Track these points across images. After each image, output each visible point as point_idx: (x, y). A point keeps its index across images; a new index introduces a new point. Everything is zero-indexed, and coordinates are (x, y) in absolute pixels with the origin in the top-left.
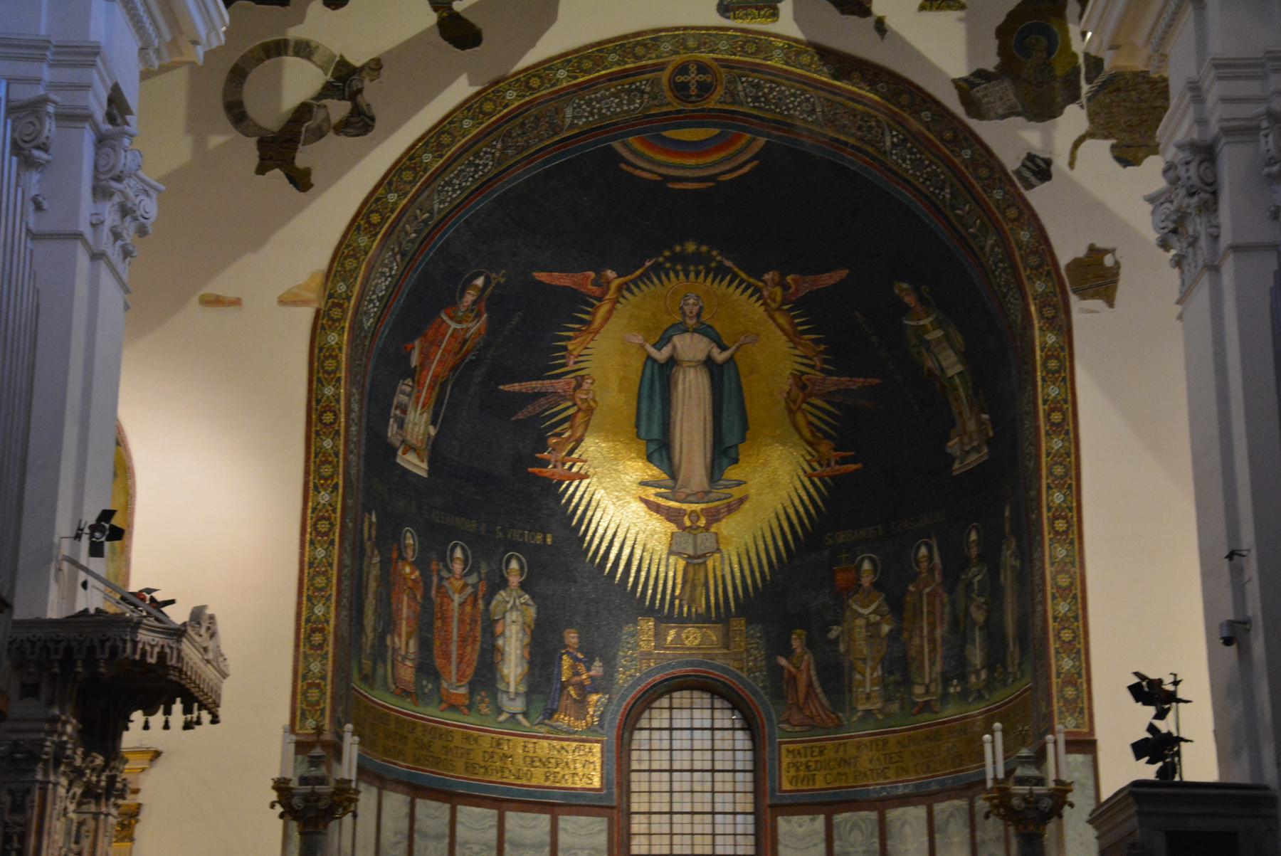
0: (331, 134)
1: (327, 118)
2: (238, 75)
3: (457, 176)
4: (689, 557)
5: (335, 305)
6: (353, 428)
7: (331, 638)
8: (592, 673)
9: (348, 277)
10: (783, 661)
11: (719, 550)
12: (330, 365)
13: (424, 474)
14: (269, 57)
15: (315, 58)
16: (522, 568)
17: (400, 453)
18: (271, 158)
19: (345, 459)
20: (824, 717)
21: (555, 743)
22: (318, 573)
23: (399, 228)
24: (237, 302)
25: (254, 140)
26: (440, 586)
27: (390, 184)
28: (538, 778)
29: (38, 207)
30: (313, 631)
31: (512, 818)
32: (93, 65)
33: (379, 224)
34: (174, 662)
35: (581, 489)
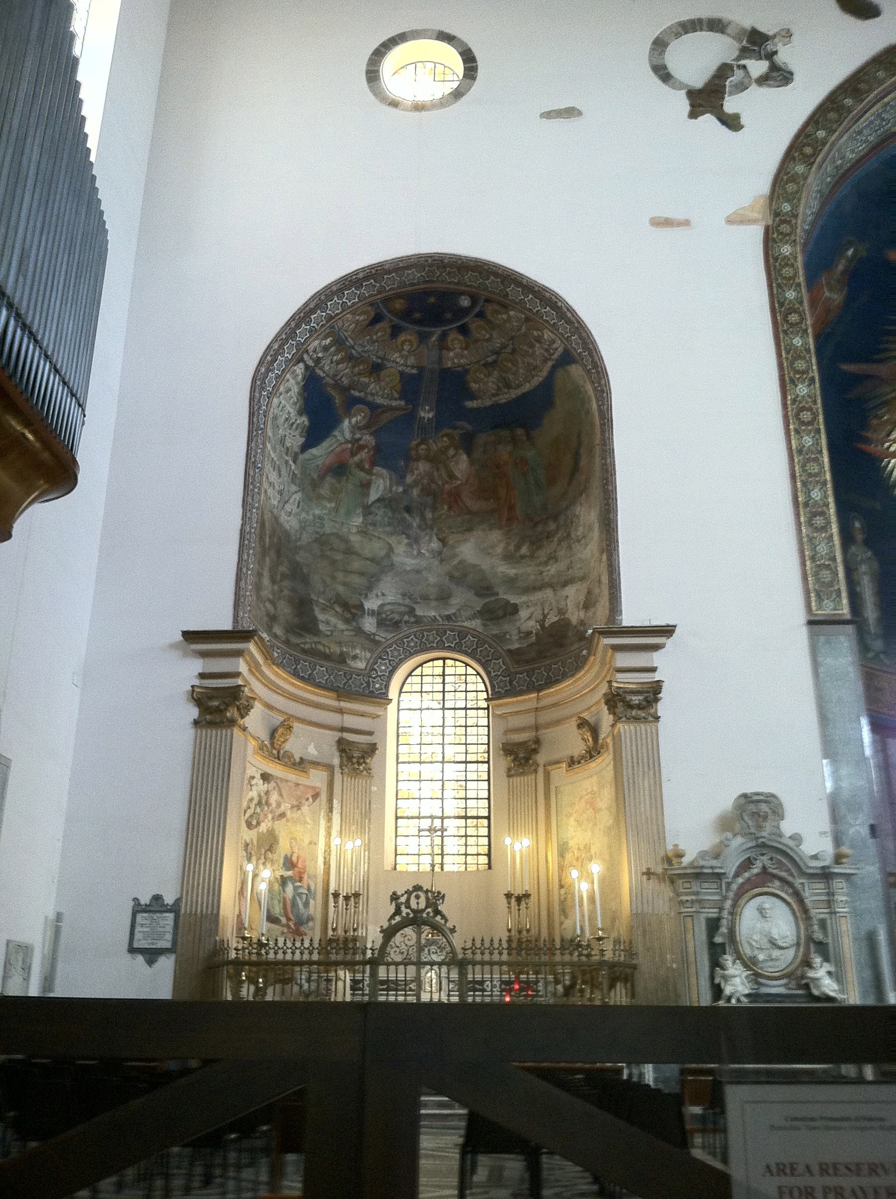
0: (754, 87)
2: (660, 45)
3: (868, 125)
7: (833, 519)
9: (792, 198)
12: (787, 272)
14: (686, 33)
15: (729, 31)
18: (701, 105)
22: (809, 460)
24: (686, 223)
25: (683, 93)
27: (817, 123)
30: (814, 515)
33: (812, 156)
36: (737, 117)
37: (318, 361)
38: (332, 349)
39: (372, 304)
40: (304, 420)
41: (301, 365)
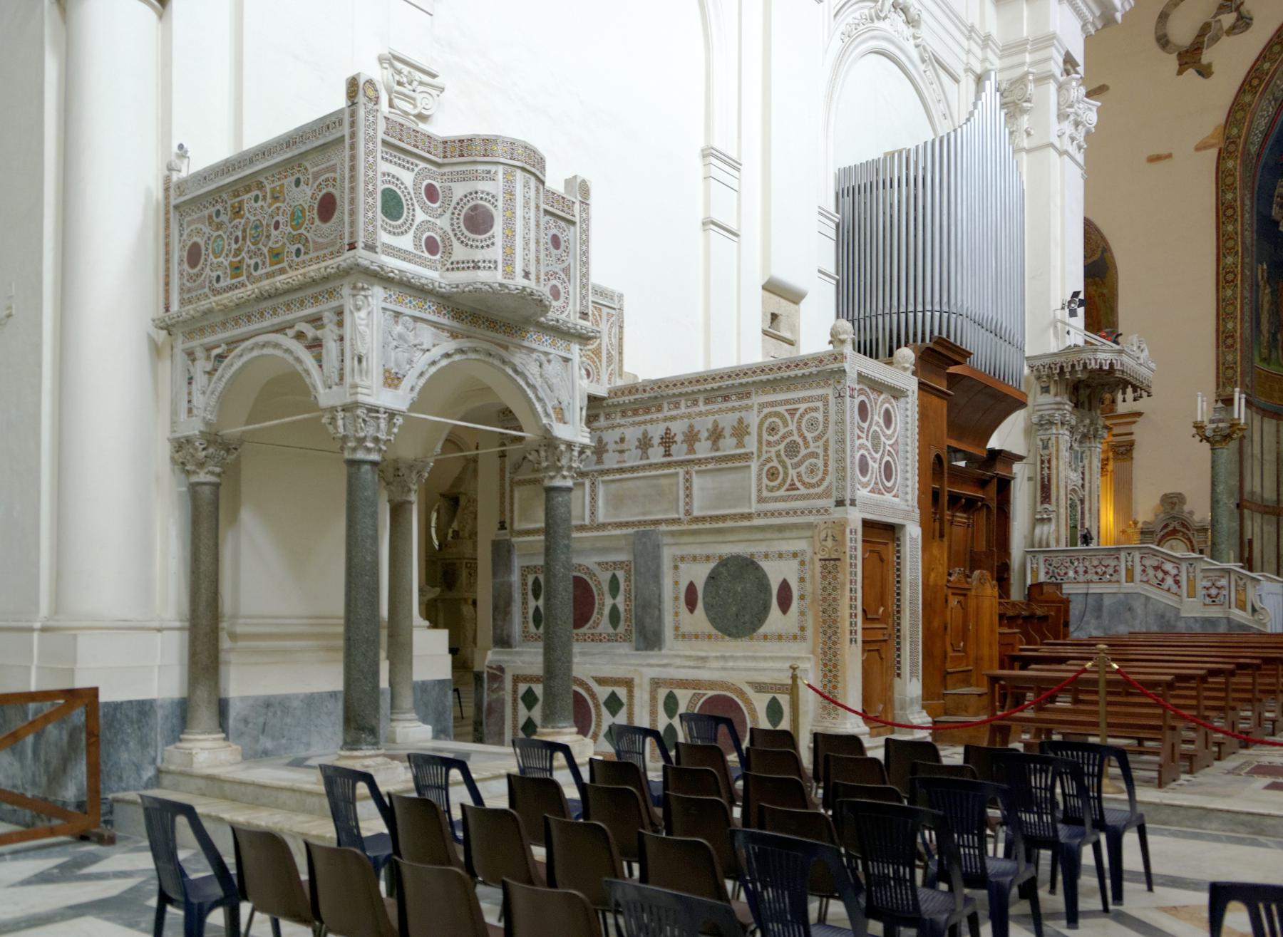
1: (1221, 28)
2: (1164, 17)
5: (1230, 143)
6: (1247, 216)
7: (1239, 340)
12: (1229, 180)
18: (1186, 63)
19: (1242, 235)
23: (1272, 84)
25: (1174, 56)
27: (1264, 57)
29: (1029, 134)
30: (1227, 337)
32: (1053, 45)
34: (1119, 367)
36: (1209, 65)
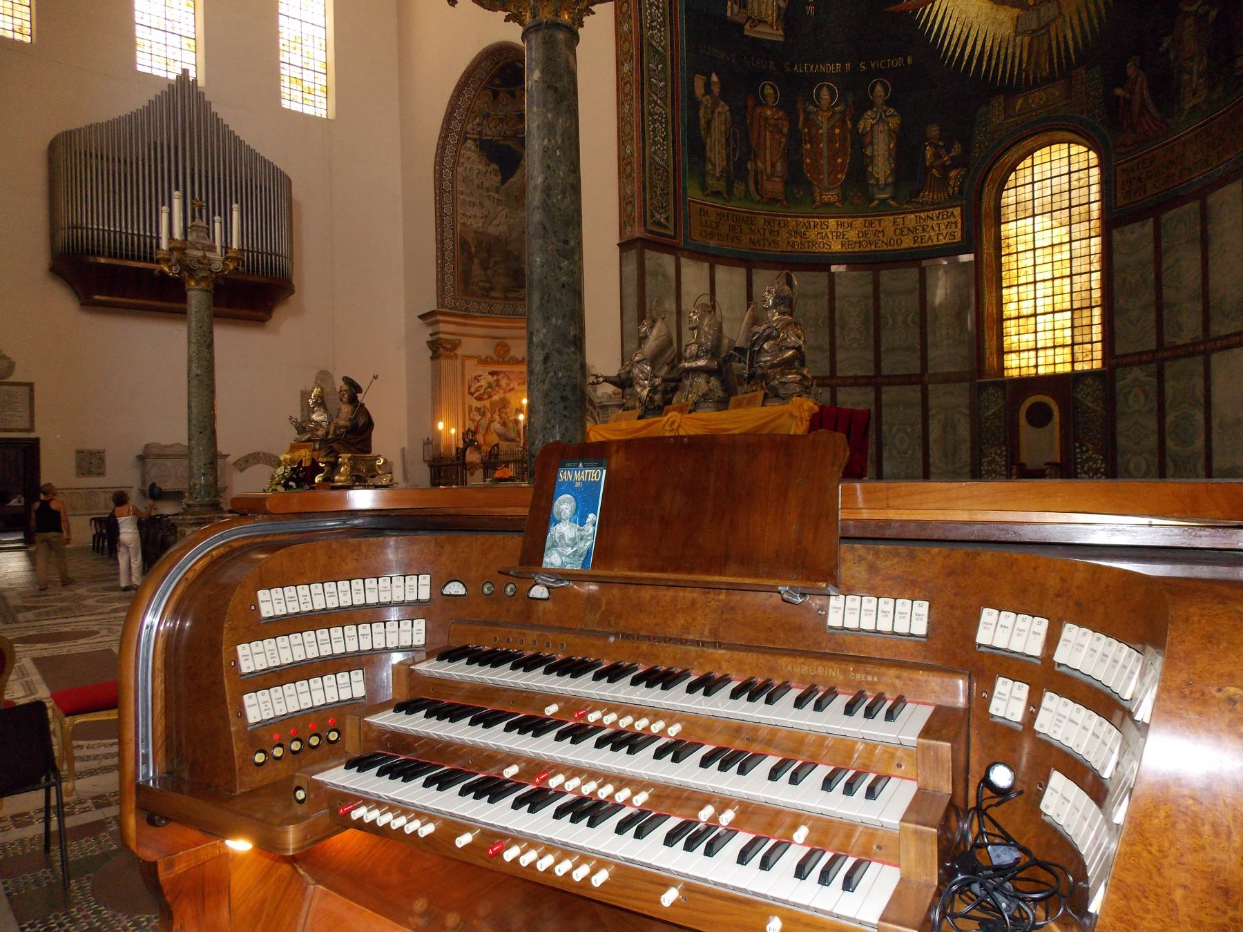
4: (1034, 31)
8: (952, 154)
10: (1118, 92)
11: (1060, 13)
13: (783, 40)
16: (886, 89)
17: (747, 26)
20: (1154, 128)
21: (922, 214)
26: (807, 121)
28: (907, 243)
31: (886, 276)
35: (935, 9)
37: (480, 133)
38: (485, 122)
39: (485, 88)
40: (494, 166)
41: (469, 141)
